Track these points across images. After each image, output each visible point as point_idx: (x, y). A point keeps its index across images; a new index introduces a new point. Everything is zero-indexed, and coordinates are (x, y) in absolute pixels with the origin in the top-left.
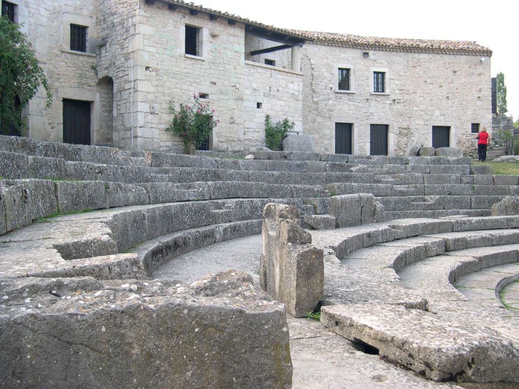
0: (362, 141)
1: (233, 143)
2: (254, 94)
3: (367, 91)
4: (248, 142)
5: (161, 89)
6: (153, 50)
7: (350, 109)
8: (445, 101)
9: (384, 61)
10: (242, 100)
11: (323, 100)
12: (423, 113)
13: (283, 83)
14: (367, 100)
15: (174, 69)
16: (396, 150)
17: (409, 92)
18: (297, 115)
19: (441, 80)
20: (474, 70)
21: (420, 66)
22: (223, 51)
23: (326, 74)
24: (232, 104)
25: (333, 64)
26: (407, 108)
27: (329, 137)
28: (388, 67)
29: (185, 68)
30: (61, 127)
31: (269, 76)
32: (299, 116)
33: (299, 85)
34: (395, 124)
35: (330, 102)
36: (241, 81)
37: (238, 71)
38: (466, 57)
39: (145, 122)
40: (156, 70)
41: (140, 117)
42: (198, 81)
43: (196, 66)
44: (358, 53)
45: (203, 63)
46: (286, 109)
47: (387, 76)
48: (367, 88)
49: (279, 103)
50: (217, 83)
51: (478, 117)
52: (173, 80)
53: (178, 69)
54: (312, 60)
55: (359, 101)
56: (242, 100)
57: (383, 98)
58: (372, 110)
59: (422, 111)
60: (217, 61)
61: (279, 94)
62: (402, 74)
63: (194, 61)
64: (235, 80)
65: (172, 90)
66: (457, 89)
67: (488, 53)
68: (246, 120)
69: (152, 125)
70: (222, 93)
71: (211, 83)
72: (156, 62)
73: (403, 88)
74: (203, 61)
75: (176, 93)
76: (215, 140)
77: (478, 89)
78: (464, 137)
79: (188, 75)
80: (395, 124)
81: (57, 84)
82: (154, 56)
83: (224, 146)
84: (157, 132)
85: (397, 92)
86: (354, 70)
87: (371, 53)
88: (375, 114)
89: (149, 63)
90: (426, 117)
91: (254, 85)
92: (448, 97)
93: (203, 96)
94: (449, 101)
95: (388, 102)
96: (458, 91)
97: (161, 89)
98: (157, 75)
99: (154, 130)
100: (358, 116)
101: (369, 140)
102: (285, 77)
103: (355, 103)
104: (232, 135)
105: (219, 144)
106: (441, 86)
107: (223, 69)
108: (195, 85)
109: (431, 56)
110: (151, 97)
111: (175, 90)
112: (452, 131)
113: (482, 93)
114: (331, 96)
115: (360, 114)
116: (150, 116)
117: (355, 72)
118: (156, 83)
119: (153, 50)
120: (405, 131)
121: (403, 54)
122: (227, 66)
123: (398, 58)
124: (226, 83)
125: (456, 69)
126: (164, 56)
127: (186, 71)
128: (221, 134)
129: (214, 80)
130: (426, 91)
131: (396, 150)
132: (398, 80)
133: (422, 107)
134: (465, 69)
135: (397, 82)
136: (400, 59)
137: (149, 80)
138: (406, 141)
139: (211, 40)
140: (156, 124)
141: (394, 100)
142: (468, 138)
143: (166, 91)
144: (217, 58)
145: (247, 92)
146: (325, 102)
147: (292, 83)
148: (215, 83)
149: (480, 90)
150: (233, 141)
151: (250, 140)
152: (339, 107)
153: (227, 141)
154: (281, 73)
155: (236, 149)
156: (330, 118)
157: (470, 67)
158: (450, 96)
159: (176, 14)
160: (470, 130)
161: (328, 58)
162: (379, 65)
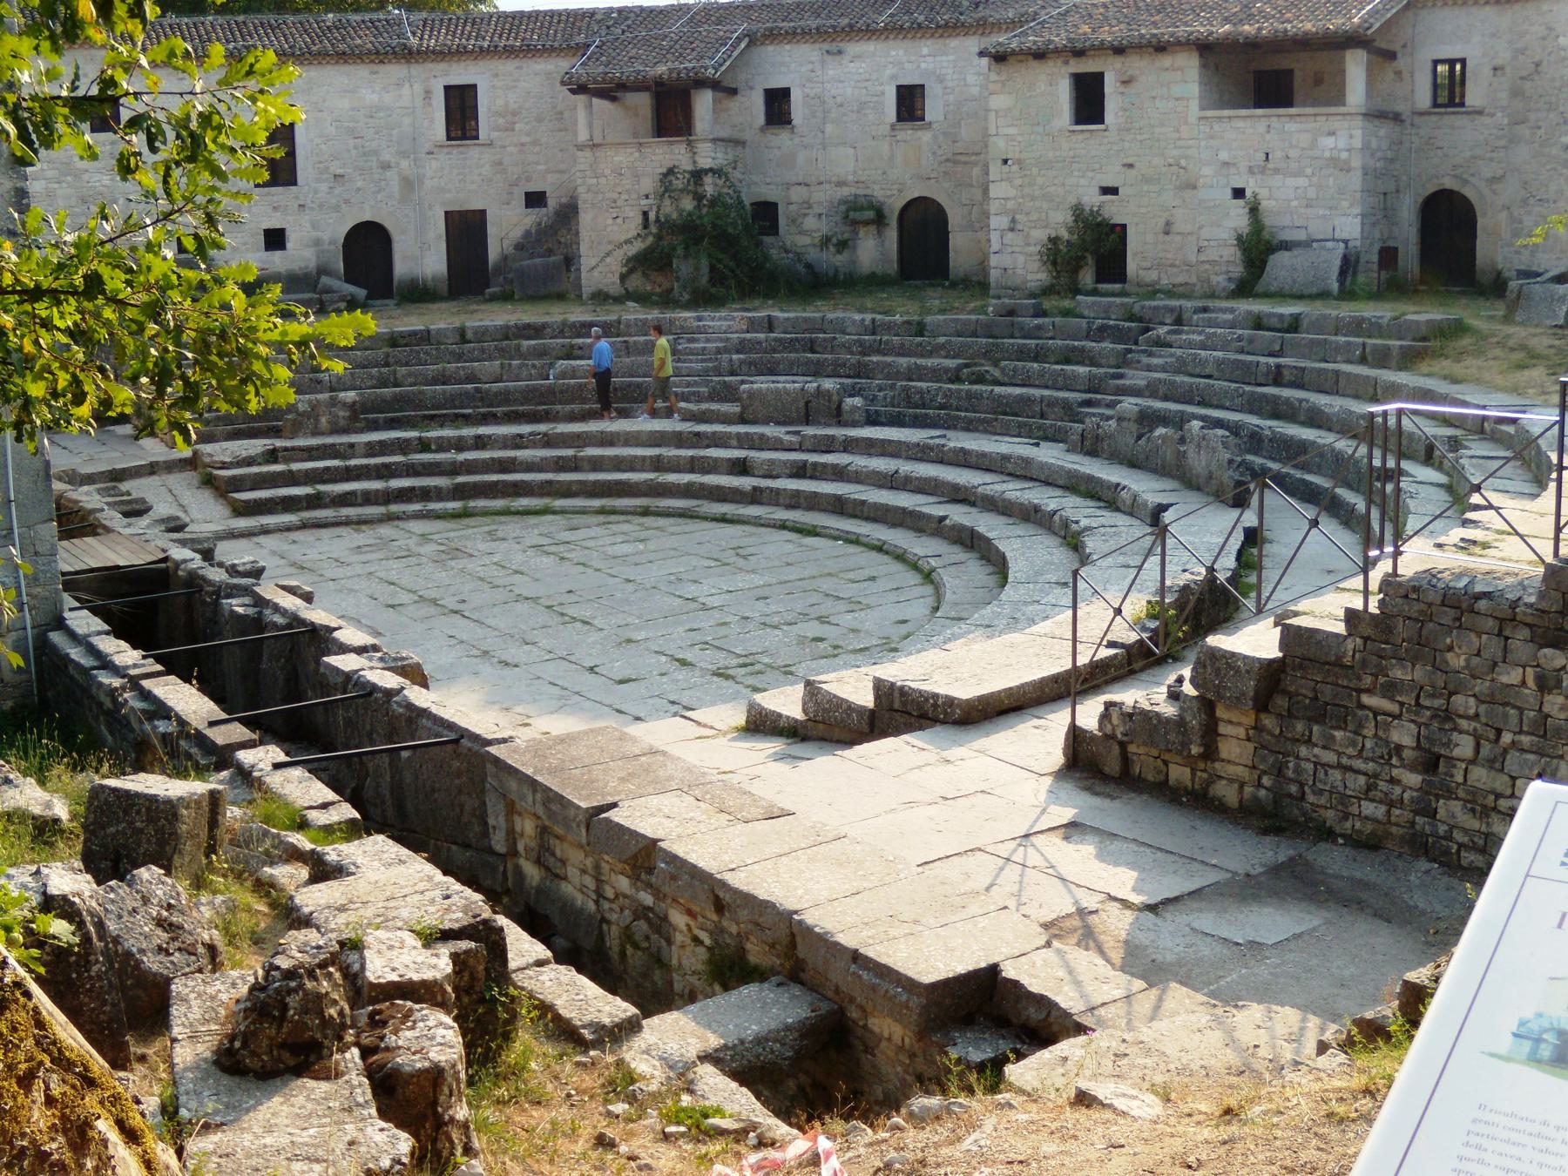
6: (1012, 131)
10: (1195, 187)
13: (1305, 139)
15: (1050, 155)
18: (1345, 204)
32: (1352, 205)
33: (1351, 137)
36: (1190, 152)
40: (1019, 162)
41: (995, 237)
46: (1312, 193)
49: (1291, 182)
50: (1137, 165)
56: (1195, 187)
64: (1176, 152)
70: (1147, 180)
83: (1152, 276)
91: (1224, 156)
93: (1113, 191)
97: (1027, 190)
102: (1310, 125)
104: (1169, 256)
108: (1091, 174)
110: (1010, 205)
111: (1053, 189)
116: (1010, 235)
118: (1018, 182)
119: (1012, 131)
122: (1157, 130)
129: (1130, 160)
139: (1121, 89)
143: (1037, 193)
145: (1207, 171)
147: (1332, 133)
148: (1131, 166)
150: (1172, 265)
151: (1212, 262)
155: (1180, 279)
159: (1051, 63)
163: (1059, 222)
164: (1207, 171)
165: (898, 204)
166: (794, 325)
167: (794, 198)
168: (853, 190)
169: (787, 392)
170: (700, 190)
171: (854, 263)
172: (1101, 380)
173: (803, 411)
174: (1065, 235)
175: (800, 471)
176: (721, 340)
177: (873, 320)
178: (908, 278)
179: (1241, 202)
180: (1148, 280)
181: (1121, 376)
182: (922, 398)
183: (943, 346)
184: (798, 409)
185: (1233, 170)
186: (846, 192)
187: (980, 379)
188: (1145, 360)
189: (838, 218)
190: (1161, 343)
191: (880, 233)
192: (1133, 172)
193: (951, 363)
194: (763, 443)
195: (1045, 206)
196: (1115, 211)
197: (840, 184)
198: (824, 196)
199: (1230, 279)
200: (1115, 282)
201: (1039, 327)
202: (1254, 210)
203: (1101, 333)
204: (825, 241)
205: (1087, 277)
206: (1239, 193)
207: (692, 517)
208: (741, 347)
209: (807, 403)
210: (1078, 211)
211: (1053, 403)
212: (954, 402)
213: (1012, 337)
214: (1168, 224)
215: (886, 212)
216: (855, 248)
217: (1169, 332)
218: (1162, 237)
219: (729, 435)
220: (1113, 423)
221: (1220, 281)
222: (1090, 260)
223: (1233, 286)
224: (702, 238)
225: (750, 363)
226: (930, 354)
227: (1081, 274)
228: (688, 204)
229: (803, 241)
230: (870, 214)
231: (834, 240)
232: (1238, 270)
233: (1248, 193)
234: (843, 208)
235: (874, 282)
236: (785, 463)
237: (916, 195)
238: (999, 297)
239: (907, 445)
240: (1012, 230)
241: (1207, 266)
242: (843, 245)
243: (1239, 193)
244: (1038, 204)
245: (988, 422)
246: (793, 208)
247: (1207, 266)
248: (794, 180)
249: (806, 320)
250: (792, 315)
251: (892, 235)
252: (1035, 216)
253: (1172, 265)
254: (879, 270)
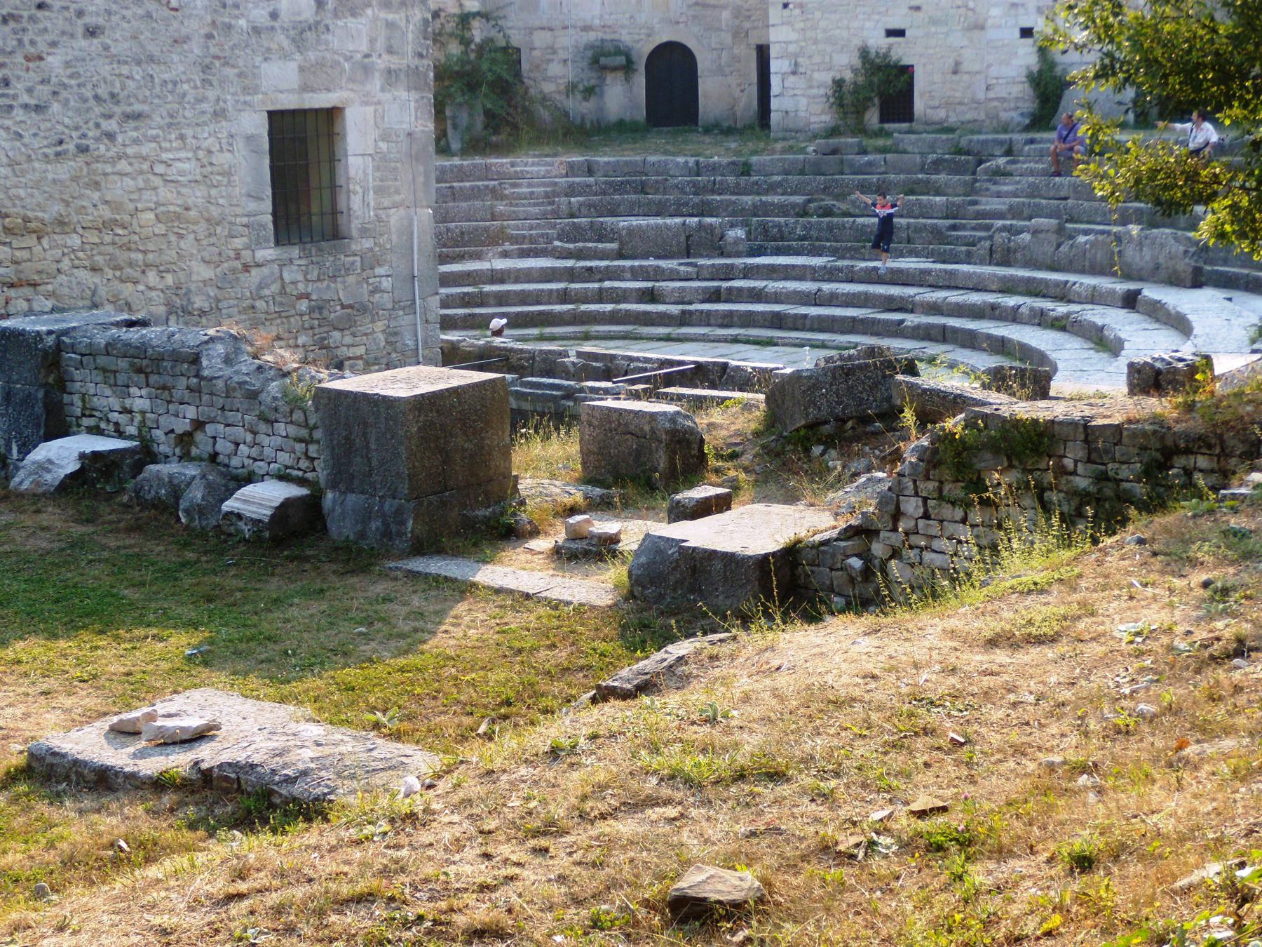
1: (959, 108)
2: (1013, 12)
10: (982, 28)
24: (957, 39)
30: (755, 88)
40: (801, 6)
42: (882, 9)
50: (924, 7)
52: (833, 17)
56: (982, 28)
69: (796, 92)
70: (934, 22)
71: (911, 8)
76: (919, 105)
81: (747, 25)
93: (900, 33)
97: (810, 34)
104: (958, 94)
105: (929, 111)
108: (877, 17)
110: (792, 48)
111: (838, 31)
116: (792, 79)
118: (801, 25)
137: (788, 23)
143: (820, 36)
145: (995, 12)
148: (918, 8)
150: (961, 103)
153: (948, 104)
155: (968, 116)
163: (845, 64)
164: (995, 12)
165: (645, 49)
166: (615, 168)
167: (537, 43)
168: (600, 35)
169: (668, 228)
170: (467, 35)
171: (601, 109)
172: (959, 206)
173: (684, 245)
174: (848, 76)
175: (715, 296)
176: (544, 185)
177: (697, 163)
178: (656, 125)
179: (1029, 41)
180: (936, 118)
181: (975, 203)
182: (780, 231)
183: (780, 184)
184: (679, 244)
185: (1021, 10)
186: (592, 36)
187: (828, 212)
188: (994, 188)
189: (585, 64)
190: (999, 173)
191: (627, 80)
192: (921, 14)
193: (799, 199)
194: (659, 275)
195: (829, 49)
196: (902, 52)
197: (586, 28)
198: (568, 41)
199: (1022, 114)
200: (900, 121)
201: (870, 164)
202: (1042, 51)
203: (937, 166)
204: (571, 88)
205: (872, 117)
206: (1026, 33)
207: (636, 339)
208: (571, 191)
209: (688, 238)
210: (864, 53)
211: (919, 229)
212: (814, 233)
213: (842, 173)
214: (957, 64)
215: (634, 58)
216: (602, 94)
217: (1008, 162)
218: (949, 77)
219: (623, 269)
220: (1026, 237)
221: (1014, 116)
222: (876, 101)
223: (1027, 121)
224: (479, 85)
225: (590, 206)
226: (766, 192)
227: (867, 116)
228: (455, 49)
229: (548, 88)
230: (621, 60)
231: (581, 87)
232: (1030, 105)
234: (589, 53)
235: (622, 130)
236: (697, 289)
237: (665, 39)
238: (784, 139)
239: (813, 269)
240: (794, 73)
241: (996, 104)
242: (589, 92)
243: (1026, 33)
244: (821, 47)
245: (856, 250)
246: (536, 53)
247: (996, 104)
248: (537, 23)
249: (626, 163)
250: (612, 159)
251: (640, 80)
252: (817, 59)
253: (961, 103)
254: (627, 117)
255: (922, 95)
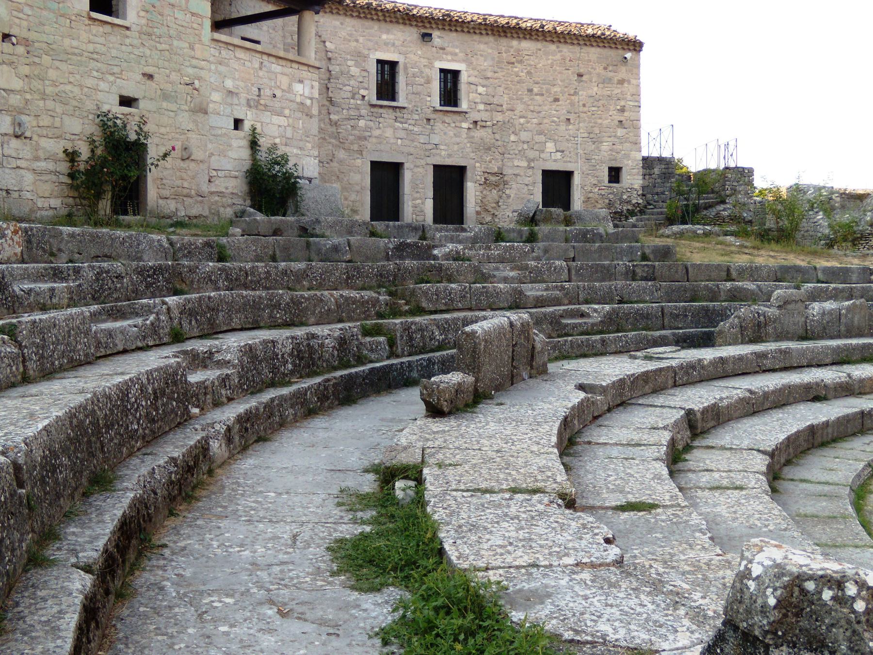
0: (418, 195)
1: (188, 201)
2: (229, 100)
3: (428, 103)
4: (217, 198)
5: (36, 84)
7: (398, 136)
8: (563, 127)
9: (457, 51)
11: (349, 119)
12: (525, 146)
13: (284, 81)
14: (428, 120)
16: (478, 213)
17: (500, 109)
18: (309, 145)
19: (557, 89)
20: (611, 74)
21: (521, 62)
22: (167, 11)
23: (355, 71)
24: (185, 120)
25: (366, 52)
26: (497, 136)
27: (358, 188)
28: (464, 61)
29: (89, 42)
31: (257, 66)
32: (313, 147)
33: (312, 87)
34: (478, 165)
35: (362, 123)
36: (203, 73)
37: (198, 54)
38: (598, 50)
39: (3, 155)
40: (26, 43)
42: (116, 70)
43: (113, 38)
44: (411, 34)
45: (128, 32)
46: (289, 134)
47: (464, 78)
48: (429, 99)
49: (276, 120)
50: (156, 76)
51: (620, 156)
52: (64, 66)
53: (75, 43)
54: (327, 44)
55: (413, 122)
56: (206, 113)
57: (457, 117)
58: (435, 139)
59: (524, 142)
60: (155, 30)
61: (277, 104)
62: (489, 74)
63: (108, 28)
64: (190, 71)
65: (62, 88)
66: (584, 105)
67: (636, 46)
68: (212, 154)
69: (19, 163)
70: (165, 97)
71: (144, 75)
72: (25, 24)
73: (491, 100)
74: (128, 28)
75: (71, 95)
76: (152, 193)
77: (619, 107)
78: (596, 190)
79: (95, 56)
80: (478, 165)
82: (21, 11)
83: (171, 206)
84: (29, 177)
85: (481, 107)
86: (405, 64)
87: (436, 34)
88: (442, 147)
89: (11, 27)
90: (531, 154)
91: (229, 84)
92: (568, 120)
94: (570, 127)
95: (465, 125)
96: (585, 109)
98: (28, 52)
99: (22, 172)
100: (412, 150)
101: (431, 194)
103: (406, 126)
104: (186, 185)
105: (161, 201)
106: (556, 100)
107: (167, 47)
108: (111, 78)
109: (539, 45)
111: (68, 88)
112: (577, 180)
113: (626, 114)
114: (363, 112)
115: (416, 147)
116: (14, 143)
117: (406, 68)
118: (26, 70)
120: (493, 179)
121: (491, 39)
122: (175, 43)
123: (482, 46)
124: (174, 76)
125: (582, 71)
126: (45, 13)
127: (91, 47)
128: (164, 181)
129: (149, 70)
130: (532, 108)
131: (478, 213)
132: (483, 86)
133: (524, 136)
134: (597, 71)
135: (481, 89)
136: (486, 47)
137: (11, 63)
138: (497, 198)
140: (27, 160)
141: (476, 122)
142: (603, 192)
143: (49, 90)
144: (156, 25)
145: (216, 97)
146: (352, 122)
148: (150, 77)
149: (622, 110)
150: (188, 196)
151: (220, 194)
152: (377, 133)
153: (176, 196)
154: (281, 62)
155: (194, 212)
156: (361, 152)
157: (605, 68)
158: (572, 117)
160: (606, 179)
161: (357, 41)
162: (449, 57)
180: (167, 211)
195: (59, 109)
205: (105, 206)
233: (247, 125)
252: (45, 121)
253: (188, 196)
255: (154, 180)
